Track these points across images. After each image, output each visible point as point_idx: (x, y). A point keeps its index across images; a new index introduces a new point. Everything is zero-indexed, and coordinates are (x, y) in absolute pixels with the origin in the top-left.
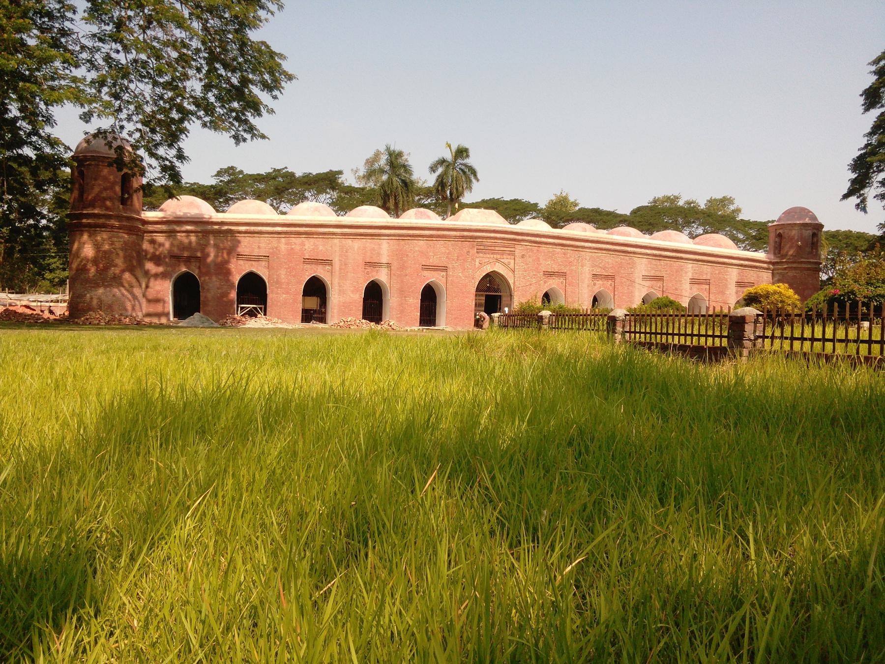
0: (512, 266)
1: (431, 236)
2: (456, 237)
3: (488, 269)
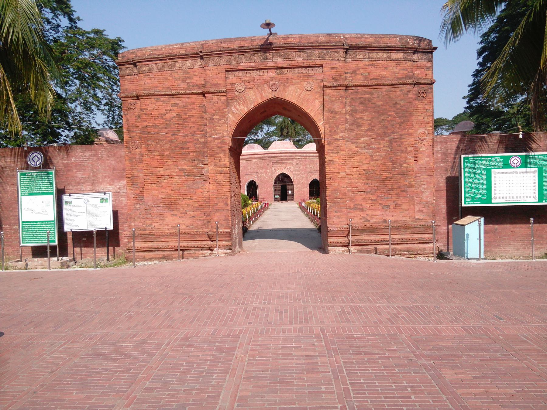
0: (292, 169)
1: (248, 158)
2: (261, 158)
3: (280, 172)
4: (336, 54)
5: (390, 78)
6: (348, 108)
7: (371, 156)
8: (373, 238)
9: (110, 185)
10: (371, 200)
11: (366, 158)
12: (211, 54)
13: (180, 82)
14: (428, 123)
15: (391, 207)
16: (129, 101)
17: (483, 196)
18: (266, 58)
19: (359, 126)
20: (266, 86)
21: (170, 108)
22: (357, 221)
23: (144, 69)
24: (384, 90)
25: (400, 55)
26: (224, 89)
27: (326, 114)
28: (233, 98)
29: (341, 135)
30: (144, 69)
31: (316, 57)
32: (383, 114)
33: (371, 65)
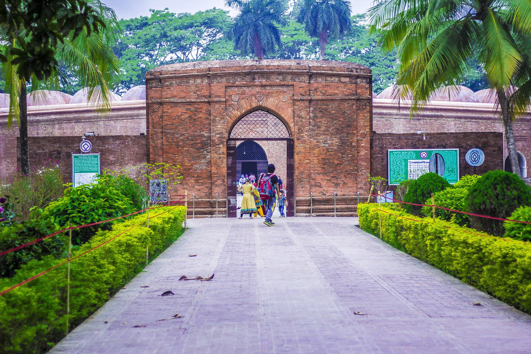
4: (303, 78)
5: (340, 95)
6: (311, 115)
7: (327, 149)
8: (327, 207)
9: (134, 166)
10: (327, 180)
11: (323, 150)
12: (215, 76)
13: (192, 94)
14: (367, 126)
15: (341, 185)
16: (154, 106)
17: (402, 178)
18: (254, 79)
19: (319, 127)
20: (253, 98)
21: (184, 111)
22: (317, 195)
23: (167, 83)
24: (336, 104)
25: (347, 80)
26: (224, 100)
27: (296, 118)
28: (230, 105)
29: (306, 133)
30: (167, 83)
31: (289, 80)
32: (335, 119)
33: (327, 85)
